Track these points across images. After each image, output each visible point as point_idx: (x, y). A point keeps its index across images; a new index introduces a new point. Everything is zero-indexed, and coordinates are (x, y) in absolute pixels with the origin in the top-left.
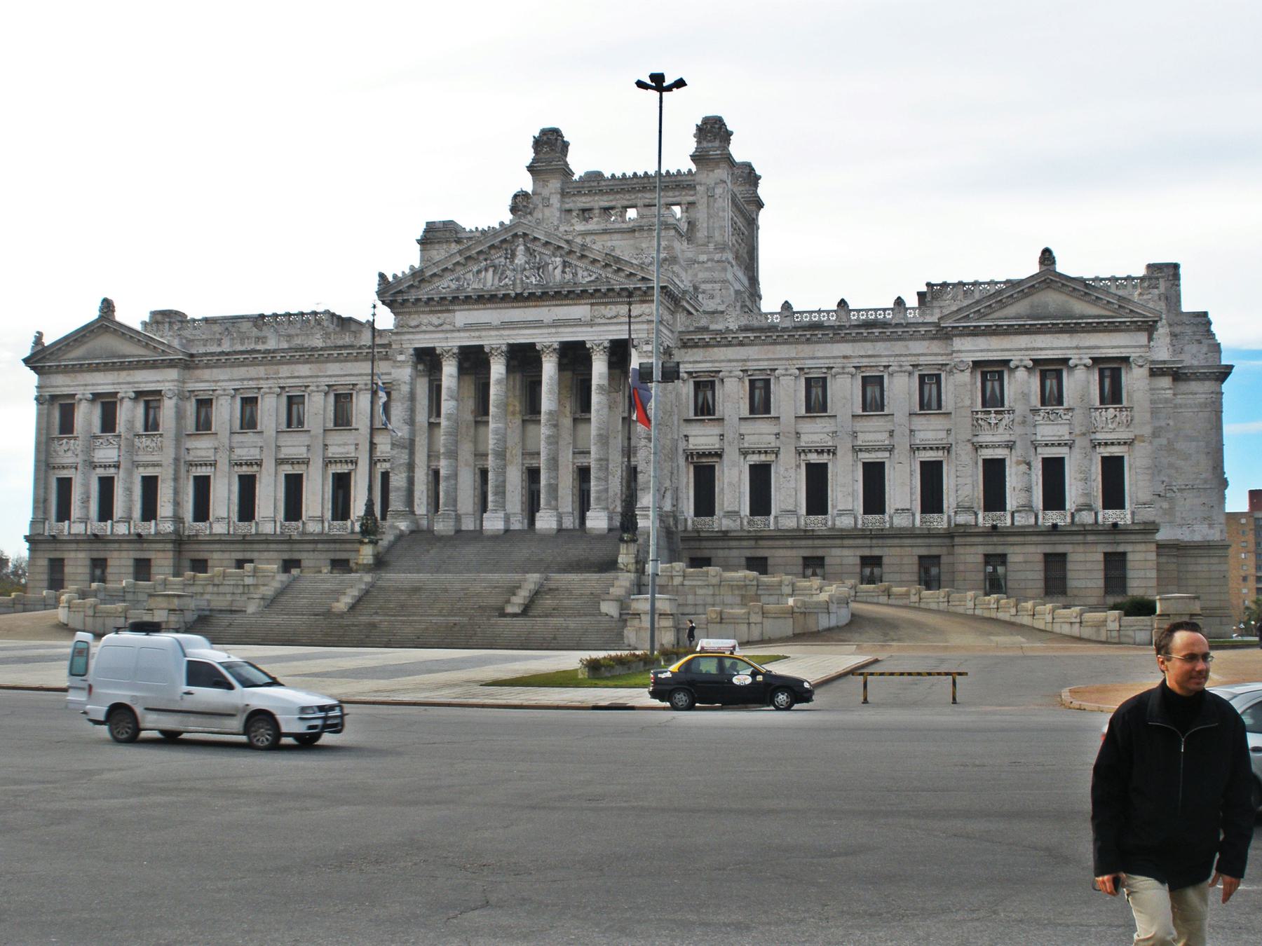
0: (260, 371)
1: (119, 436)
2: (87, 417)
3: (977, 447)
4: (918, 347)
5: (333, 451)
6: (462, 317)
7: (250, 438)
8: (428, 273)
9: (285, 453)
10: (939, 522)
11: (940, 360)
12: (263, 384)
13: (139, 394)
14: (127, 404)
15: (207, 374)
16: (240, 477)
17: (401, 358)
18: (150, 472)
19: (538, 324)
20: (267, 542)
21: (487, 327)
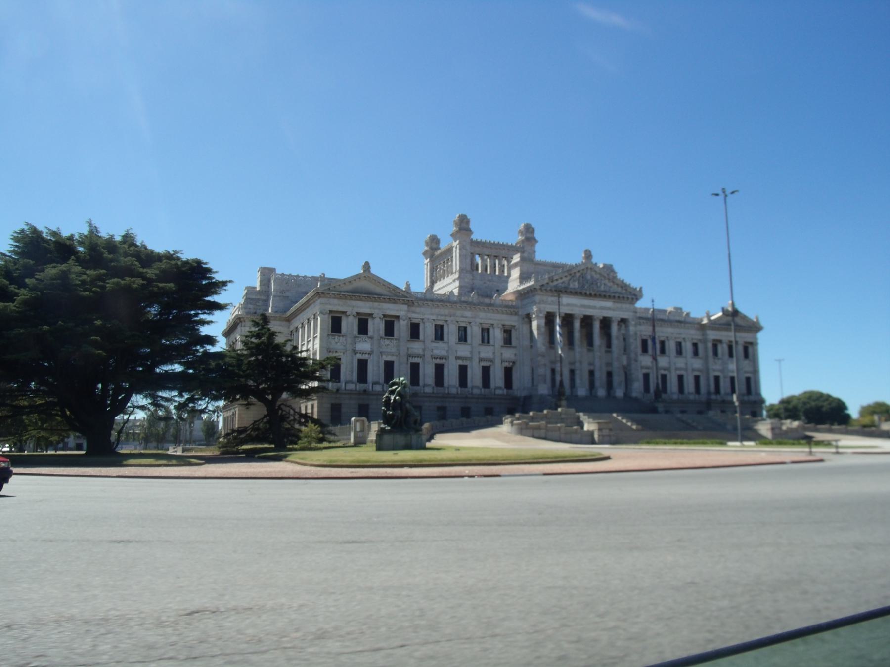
0: (447, 311)
1: (371, 338)
2: (349, 325)
3: (714, 370)
4: (693, 332)
5: (483, 355)
6: (566, 300)
7: (440, 344)
8: (555, 278)
9: (460, 354)
10: (703, 397)
11: (700, 338)
12: (447, 318)
13: (385, 316)
14: (377, 320)
15: (418, 310)
16: (436, 365)
17: (541, 315)
18: (389, 358)
19: (594, 308)
20: (454, 397)
21: (575, 306)
